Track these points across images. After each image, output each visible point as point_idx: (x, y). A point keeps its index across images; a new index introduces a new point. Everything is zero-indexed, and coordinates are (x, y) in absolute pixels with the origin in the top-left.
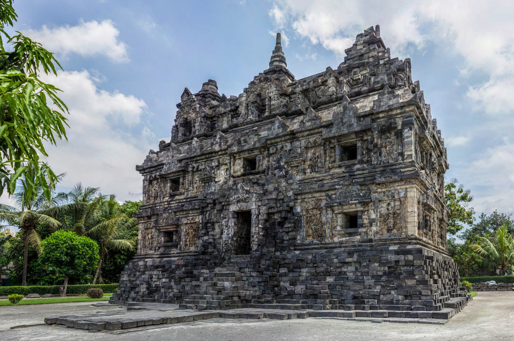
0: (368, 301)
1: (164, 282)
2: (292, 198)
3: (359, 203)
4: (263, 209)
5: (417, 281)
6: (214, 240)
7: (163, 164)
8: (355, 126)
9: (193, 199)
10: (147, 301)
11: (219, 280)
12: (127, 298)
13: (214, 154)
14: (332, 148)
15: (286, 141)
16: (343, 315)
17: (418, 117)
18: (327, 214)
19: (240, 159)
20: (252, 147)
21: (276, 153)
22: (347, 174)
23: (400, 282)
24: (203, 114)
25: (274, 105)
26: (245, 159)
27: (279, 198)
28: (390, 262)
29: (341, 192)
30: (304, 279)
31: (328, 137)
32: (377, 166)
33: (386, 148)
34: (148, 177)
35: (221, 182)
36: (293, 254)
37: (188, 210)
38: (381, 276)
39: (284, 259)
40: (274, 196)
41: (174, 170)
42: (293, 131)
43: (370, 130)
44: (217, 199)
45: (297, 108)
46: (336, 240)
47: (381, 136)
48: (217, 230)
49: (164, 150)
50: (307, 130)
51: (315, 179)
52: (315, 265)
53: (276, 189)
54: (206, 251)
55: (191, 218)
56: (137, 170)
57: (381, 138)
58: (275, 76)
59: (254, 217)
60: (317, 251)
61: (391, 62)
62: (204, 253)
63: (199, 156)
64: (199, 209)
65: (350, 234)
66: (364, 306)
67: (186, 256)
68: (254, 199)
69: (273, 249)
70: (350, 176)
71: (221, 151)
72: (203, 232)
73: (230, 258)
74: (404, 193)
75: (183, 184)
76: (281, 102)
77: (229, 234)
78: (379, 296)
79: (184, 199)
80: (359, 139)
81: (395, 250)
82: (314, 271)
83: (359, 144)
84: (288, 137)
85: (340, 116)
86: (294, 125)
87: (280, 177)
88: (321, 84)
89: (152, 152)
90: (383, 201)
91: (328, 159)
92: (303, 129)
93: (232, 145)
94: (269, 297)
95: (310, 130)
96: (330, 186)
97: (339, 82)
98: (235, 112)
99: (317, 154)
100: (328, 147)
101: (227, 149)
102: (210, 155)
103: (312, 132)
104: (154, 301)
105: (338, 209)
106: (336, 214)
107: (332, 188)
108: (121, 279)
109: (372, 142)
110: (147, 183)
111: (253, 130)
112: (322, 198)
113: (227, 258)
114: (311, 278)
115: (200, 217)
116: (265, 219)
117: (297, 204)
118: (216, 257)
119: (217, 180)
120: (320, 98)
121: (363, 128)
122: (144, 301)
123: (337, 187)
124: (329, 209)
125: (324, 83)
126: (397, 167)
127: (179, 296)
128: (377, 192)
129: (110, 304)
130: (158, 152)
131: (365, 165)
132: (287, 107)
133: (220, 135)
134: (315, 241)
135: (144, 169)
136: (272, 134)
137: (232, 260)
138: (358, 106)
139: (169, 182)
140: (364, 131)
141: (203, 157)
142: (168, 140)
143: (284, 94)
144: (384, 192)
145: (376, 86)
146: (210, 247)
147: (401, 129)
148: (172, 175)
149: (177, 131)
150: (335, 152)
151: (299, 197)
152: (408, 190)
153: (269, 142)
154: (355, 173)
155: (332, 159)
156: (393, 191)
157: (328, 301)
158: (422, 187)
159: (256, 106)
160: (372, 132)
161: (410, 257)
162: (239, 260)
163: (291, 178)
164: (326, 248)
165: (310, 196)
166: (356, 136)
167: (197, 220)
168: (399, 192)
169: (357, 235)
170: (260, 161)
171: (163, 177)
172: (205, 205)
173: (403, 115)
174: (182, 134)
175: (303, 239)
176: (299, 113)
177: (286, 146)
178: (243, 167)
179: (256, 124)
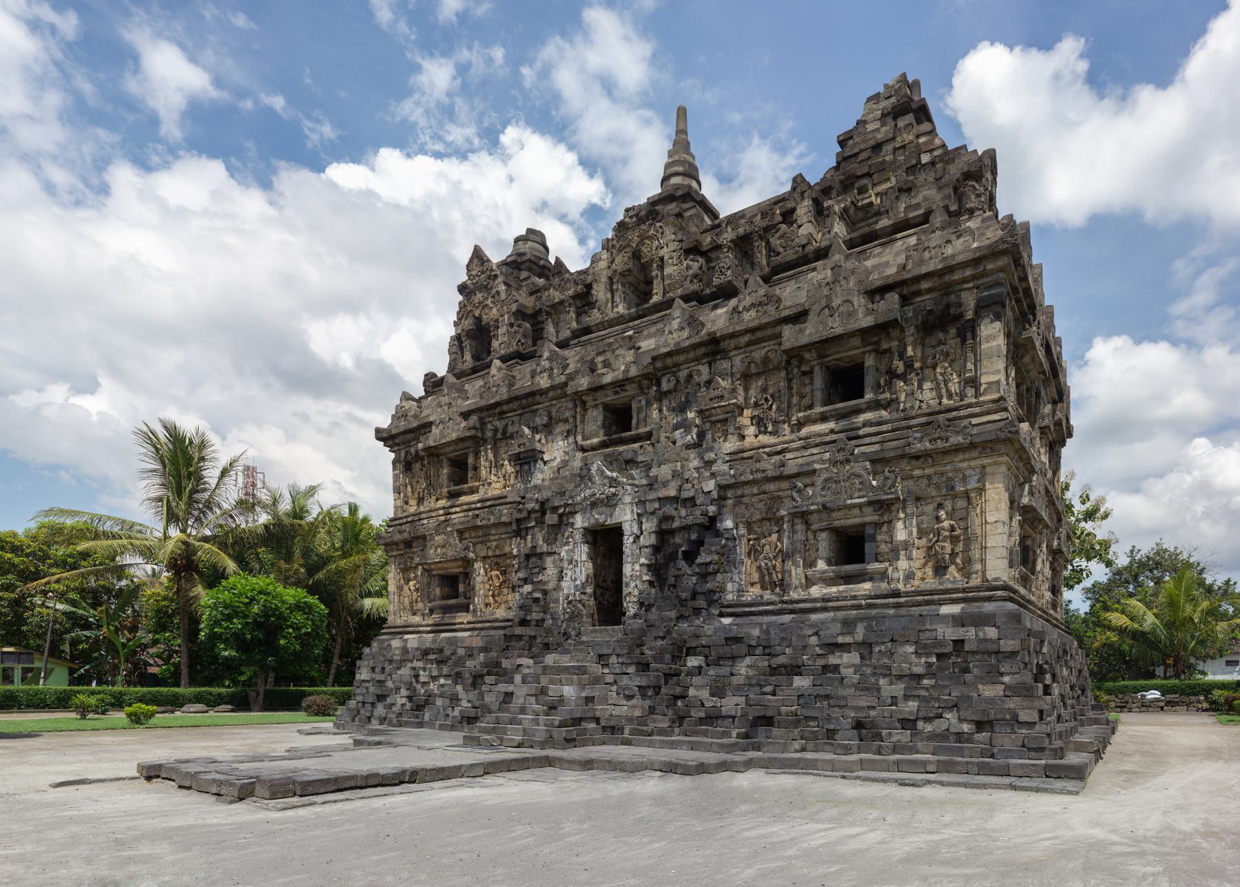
0: (890, 735)
1: (442, 686)
2: (715, 495)
4: (649, 525)
5: (1008, 687)
6: (545, 592)
7: (431, 423)
8: (860, 315)
10: (407, 724)
11: (552, 682)
12: (369, 718)
13: (538, 397)
14: (805, 373)
15: (697, 360)
16: (833, 767)
17: (1015, 290)
18: (794, 532)
19: (596, 406)
20: (621, 377)
21: (675, 390)
22: (842, 435)
23: (965, 690)
24: (514, 307)
25: (670, 276)
26: (607, 408)
27: (685, 495)
28: (941, 643)
29: (826, 480)
30: (742, 682)
31: (797, 345)
32: (914, 413)
33: (934, 368)
34: (403, 454)
35: (555, 464)
36: (717, 624)
37: (487, 527)
38: (920, 677)
39: (697, 636)
40: (673, 493)
41: (454, 436)
42: (715, 333)
43: (894, 323)
44: (548, 500)
45: (723, 279)
46: (816, 591)
47: (923, 339)
48: (551, 571)
49: (432, 393)
50: (747, 331)
51: (767, 450)
52: (767, 651)
53: (675, 475)
54: (529, 618)
55: (494, 544)
56: (378, 438)
57: (923, 345)
58: (672, 207)
59: (628, 541)
60: (773, 618)
61: (949, 156)
62: (524, 623)
63: (508, 402)
64: (510, 524)
65: (848, 579)
66: (880, 746)
68: (627, 499)
69: (673, 614)
70: (850, 439)
71: (553, 388)
72: (521, 575)
73: (578, 634)
74: (976, 478)
75: (476, 468)
76: (688, 268)
77: (575, 580)
78: (915, 721)
79: (479, 501)
80: (869, 348)
81: (953, 616)
82: (766, 664)
83: (869, 362)
84: (702, 350)
85: (825, 291)
86: (717, 319)
87: (688, 447)
88: (780, 218)
89: (406, 397)
90: (925, 499)
91: (795, 400)
92: (738, 328)
93: (577, 372)
94: (663, 721)
95: (752, 330)
96: (801, 465)
97: (820, 213)
98: (584, 299)
99: (771, 391)
100: (796, 371)
101: (566, 384)
102: (530, 399)
103: (759, 334)
104: (421, 725)
105: (820, 520)
106: (815, 532)
107: (805, 469)
108: (358, 677)
109: (902, 355)
110: (401, 466)
111: (623, 338)
112: (781, 493)
113: (573, 633)
114: (759, 680)
116: (653, 546)
117: (725, 510)
118: (549, 632)
119: (546, 457)
120: (779, 254)
121: (881, 320)
122: (400, 725)
123: (817, 466)
124: (797, 521)
125: (788, 216)
126: (962, 413)
127: (472, 715)
129: (336, 731)
130: (421, 398)
131: (884, 413)
132: (701, 281)
133: (551, 351)
134: (768, 596)
135: (392, 437)
136: (666, 344)
137: (584, 638)
138: (869, 263)
139: (445, 464)
140: (883, 328)
141: (514, 405)
142: (441, 370)
143: (693, 250)
144: (929, 477)
145: (911, 215)
146: (535, 608)
147: (972, 320)
148: (451, 448)
149: (462, 349)
150: (812, 383)
152: (989, 470)
153: (659, 364)
154: (861, 432)
155: (806, 401)
156: (950, 475)
157: (796, 731)
158: (1021, 465)
159: (631, 284)
160: (902, 330)
161: (992, 633)
162: (599, 638)
163: (711, 449)
164: (792, 612)
165: (755, 491)
166: (863, 339)
168: (964, 475)
169: (864, 581)
170: (639, 410)
171: (433, 453)
172: (524, 514)
173: (981, 281)
174: (473, 357)
175: (740, 591)
176: (727, 292)
177: (699, 373)
178: (604, 426)
179: (631, 324)
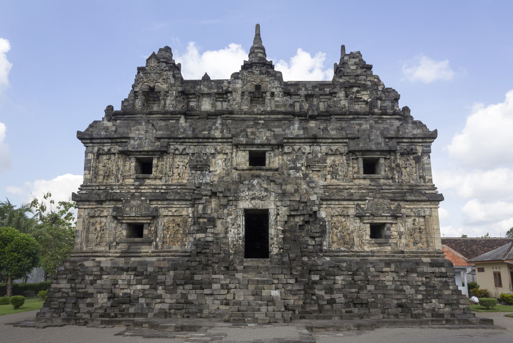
3: (391, 216)
55: (175, 209)
67: (169, 256)
119: (211, 169)
128: (405, 208)
144: (411, 209)
151: (324, 203)
167: (184, 213)
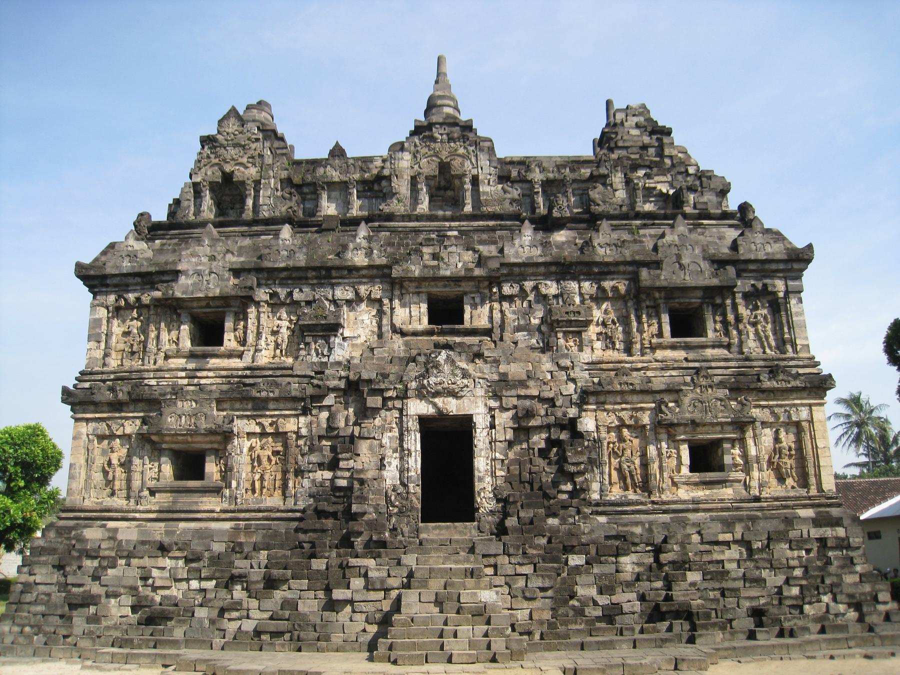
9: (279, 373)
67: (259, 519)
115: (302, 419)
